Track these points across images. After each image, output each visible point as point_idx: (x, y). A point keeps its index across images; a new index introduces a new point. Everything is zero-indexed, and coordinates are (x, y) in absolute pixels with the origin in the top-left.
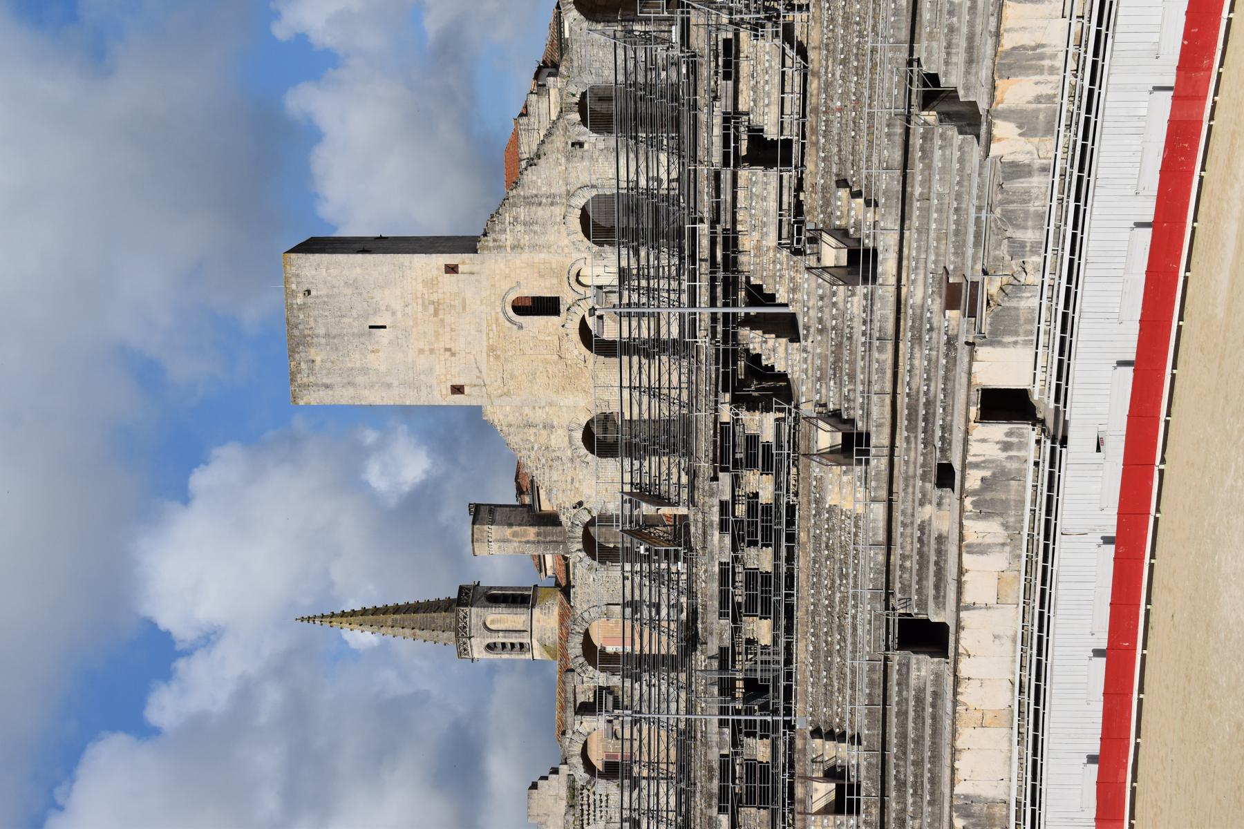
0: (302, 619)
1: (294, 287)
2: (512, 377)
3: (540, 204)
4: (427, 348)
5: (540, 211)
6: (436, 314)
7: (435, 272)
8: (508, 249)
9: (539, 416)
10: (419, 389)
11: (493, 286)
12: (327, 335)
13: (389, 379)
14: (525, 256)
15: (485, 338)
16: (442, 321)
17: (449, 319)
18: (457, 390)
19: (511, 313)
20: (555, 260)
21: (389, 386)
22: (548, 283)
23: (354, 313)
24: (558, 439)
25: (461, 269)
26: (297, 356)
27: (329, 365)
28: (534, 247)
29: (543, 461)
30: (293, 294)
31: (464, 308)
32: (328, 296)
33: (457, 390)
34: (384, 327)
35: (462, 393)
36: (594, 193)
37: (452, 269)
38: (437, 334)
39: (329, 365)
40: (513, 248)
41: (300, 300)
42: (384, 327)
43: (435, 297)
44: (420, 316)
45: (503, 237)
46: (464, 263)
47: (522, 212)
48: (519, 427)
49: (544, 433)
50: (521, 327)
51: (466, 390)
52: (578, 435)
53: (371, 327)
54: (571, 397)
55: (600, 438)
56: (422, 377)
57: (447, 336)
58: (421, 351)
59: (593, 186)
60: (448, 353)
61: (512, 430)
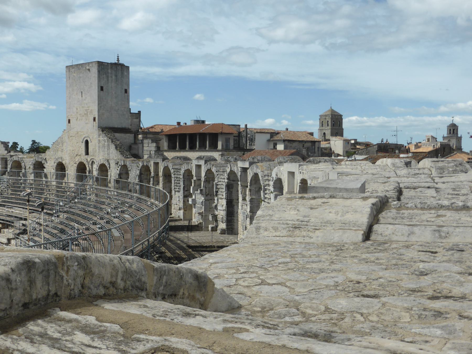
0: (118, 59)
5: (106, 150)
6: (85, 114)
9: (64, 148)
12: (80, 77)
14: (97, 144)
16: (83, 116)
17: (84, 118)
19: (85, 139)
24: (59, 154)
28: (99, 147)
30: (88, 66)
31: (86, 124)
36: (108, 168)
37: (94, 119)
38: (80, 114)
41: (88, 68)
43: (88, 114)
45: (101, 137)
47: (106, 144)
50: (82, 142)
52: (60, 161)
55: (61, 167)
58: (77, 109)
59: (110, 168)
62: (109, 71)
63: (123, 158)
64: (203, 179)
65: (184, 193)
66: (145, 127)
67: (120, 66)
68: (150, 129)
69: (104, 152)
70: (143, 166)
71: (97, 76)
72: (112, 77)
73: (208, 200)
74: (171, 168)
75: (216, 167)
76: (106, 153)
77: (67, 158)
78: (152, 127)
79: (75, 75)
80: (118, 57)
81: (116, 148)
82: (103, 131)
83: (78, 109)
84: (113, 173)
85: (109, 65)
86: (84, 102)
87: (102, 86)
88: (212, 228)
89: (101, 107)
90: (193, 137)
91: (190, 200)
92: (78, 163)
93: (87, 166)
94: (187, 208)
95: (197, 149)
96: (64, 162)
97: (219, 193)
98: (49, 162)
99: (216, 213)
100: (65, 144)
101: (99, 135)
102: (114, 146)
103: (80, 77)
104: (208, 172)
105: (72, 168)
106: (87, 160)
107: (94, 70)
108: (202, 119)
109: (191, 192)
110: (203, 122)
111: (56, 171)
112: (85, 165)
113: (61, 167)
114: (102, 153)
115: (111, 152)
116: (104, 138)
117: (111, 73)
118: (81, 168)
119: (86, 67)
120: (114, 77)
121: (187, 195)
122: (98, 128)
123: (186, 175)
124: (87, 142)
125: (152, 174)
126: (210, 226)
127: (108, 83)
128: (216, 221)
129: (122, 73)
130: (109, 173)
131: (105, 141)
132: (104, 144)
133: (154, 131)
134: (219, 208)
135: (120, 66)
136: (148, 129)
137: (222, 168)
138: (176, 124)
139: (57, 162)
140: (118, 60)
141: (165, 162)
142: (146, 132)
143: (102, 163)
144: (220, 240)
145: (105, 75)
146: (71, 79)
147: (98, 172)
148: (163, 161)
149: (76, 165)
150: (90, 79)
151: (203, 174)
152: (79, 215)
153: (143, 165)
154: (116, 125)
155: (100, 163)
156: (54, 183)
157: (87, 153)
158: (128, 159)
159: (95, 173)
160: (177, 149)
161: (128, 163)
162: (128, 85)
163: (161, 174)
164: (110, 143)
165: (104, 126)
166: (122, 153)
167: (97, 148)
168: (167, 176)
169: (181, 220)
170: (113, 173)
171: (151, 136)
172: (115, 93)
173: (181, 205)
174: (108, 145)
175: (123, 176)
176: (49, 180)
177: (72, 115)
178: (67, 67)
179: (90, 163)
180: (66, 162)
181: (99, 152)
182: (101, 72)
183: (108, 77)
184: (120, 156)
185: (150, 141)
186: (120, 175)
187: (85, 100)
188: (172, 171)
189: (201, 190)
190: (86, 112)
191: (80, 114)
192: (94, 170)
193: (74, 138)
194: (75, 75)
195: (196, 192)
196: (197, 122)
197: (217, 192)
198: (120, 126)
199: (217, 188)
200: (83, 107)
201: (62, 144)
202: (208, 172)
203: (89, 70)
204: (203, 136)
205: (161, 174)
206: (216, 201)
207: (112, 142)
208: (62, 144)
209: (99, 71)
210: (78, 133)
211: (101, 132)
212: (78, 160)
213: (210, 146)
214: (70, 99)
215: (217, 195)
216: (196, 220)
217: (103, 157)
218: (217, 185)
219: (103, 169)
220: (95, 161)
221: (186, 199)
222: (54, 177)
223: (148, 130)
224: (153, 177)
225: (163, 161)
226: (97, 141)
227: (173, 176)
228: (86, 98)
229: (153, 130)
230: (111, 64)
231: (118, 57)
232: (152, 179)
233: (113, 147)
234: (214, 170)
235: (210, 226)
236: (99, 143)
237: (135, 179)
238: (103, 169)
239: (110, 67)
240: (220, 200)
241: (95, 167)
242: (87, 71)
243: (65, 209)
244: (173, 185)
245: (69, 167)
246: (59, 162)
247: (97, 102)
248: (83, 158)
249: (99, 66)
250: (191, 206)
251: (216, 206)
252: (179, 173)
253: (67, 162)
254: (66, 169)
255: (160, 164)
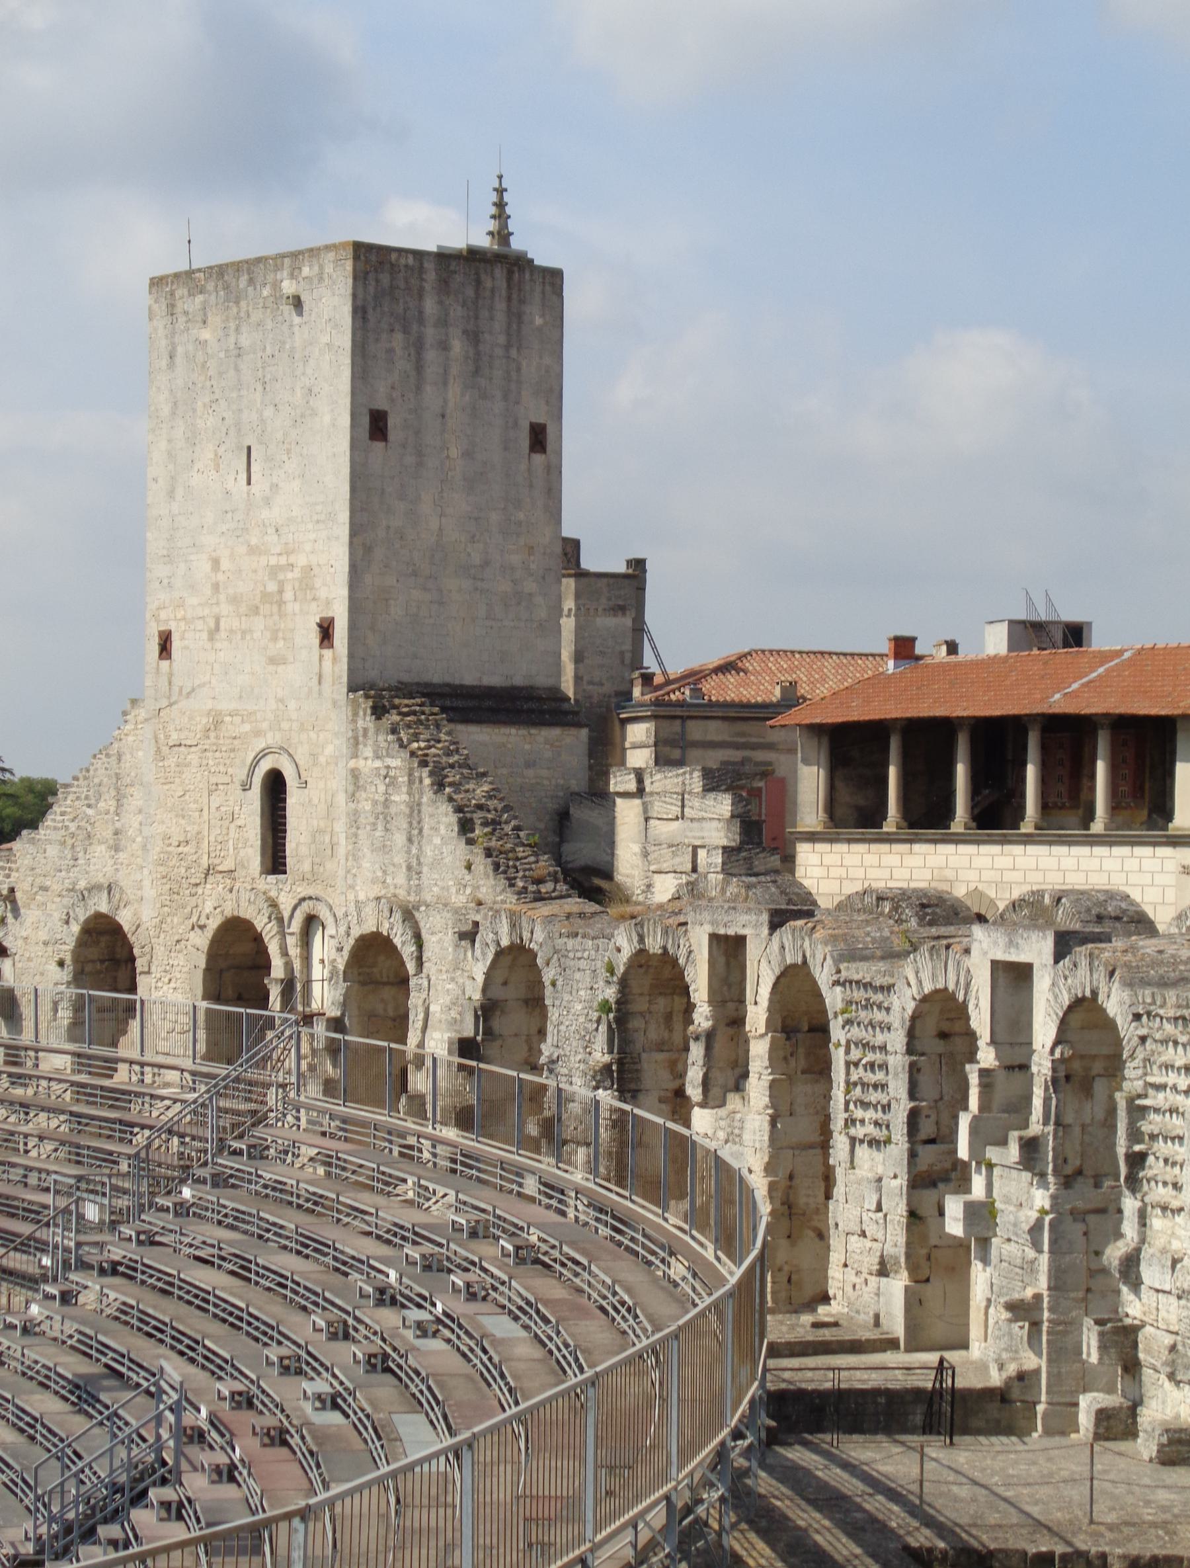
0: (501, 205)
1: (306, 271)
2: (182, 765)
3: (410, 840)
4: (221, 577)
5: (400, 839)
6: (265, 596)
7: (323, 593)
8: (352, 764)
9: (131, 821)
10: (169, 559)
11: (302, 728)
12: (239, 352)
13: (180, 492)
14: (341, 798)
15: (233, 706)
16: (255, 610)
17: (258, 623)
18: (165, 647)
19: (265, 766)
20: (335, 867)
21: (171, 494)
22: (304, 850)
23: (269, 412)
24: (99, 864)
25: (328, 653)
26: (210, 286)
27: (200, 357)
28: (354, 819)
29: (73, 827)
31: (273, 661)
32: (293, 349)
33: (165, 647)
34: (249, 483)
35: (161, 657)
36: (411, 967)
37: (326, 632)
38: (234, 600)
39: (200, 357)
40: (355, 774)
41: (288, 287)
42: (249, 483)
43: (288, 595)
44: (263, 560)
45: (368, 752)
46: (335, 660)
47: (400, 798)
48: (118, 777)
49: (108, 834)
50: (246, 787)
51: (165, 664)
52: (104, 908)
53: (249, 448)
54: (153, 893)
55: (106, 955)
56: (182, 566)
57: (235, 624)
58: (216, 563)
60: (212, 625)
61: (113, 760)
62: (430, 305)
63: (510, 900)
64: (1042, 1066)
65: (912, 1155)
66: (675, 669)
67: (499, 272)
68: (706, 686)
69: (386, 855)
70: (641, 958)
71: (344, 340)
72: (444, 346)
73: (1078, 1215)
74: (823, 976)
75: (1129, 984)
76: (399, 859)
77: (149, 892)
78: (727, 667)
79: (206, 335)
80: (500, 191)
81: (465, 827)
82: (379, 711)
83: (225, 564)
84: (445, 997)
85: (429, 265)
86: (265, 514)
87: (381, 404)
88: (1103, 1416)
89: (368, 549)
90: (997, 741)
91: (954, 1207)
92: (214, 924)
93: (273, 949)
94: (935, 1264)
95: (1027, 827)
96: (125, 919)
97: (1154, 1167)
98: (30, 915)
99: (1133, 1307)
100: (136, 799)
101: (355, 742)
102: (453, 819)
103: (239, 352)
104: (1076, 1019)
105: (179, 960)
106: (274, 905)
107: (332, 303)
108: (1070, 614)
109: (963, 1152)
110: (1075, 634)
111: (78, 978)
112: (258, 939)
113: (106, 955)
114: (369, 863)
115: (428, 851)
116: (383, 761)
117: (443, 322)
118: (237, 964)
119: (276, 286)
120: (458, 346)
121: (933, 1174)
122: (352, 689)
123: (930, 1026)
124: (275, 786)
125: (703, 1017)
126: (1088, 1405)
127: (419, 389)
128: (1132, 1367)
129: (516, 317)
130: (415, 1000)
131: (392, 783)
132: (387, 803)
133: (731, 696)
134: (1151, 1274)
135: (499, 272)
136: (694, 677)
137: (1171, 996)
138: (885, 647)
139: (82, 915)
140: (501, 211)
141: (785, 934)
142: (681, 704)
143: (369, 927)
144: (1148, 1514)
145: (399, 337)
146: (179, 360)
147: (343, 986)
148: (774, 926)
149: (202, 940)
150: (306, 359)
151: (1044, 1031)
152: (201, 1300)
153: (642, 952)
154: (472, 671)
155: (356, 932)
156: (62, 1062)
157: (275, 862)
158: (545, 909)
159: (325, 996)
160: (889, 826)
161: (539, 936)
162: (552, 391)
163: (757, 1016)
164: (428, 796)
165: (394, 675)
166: (501, 864)
167: (340, 827)
168: (803, 1029)
169: (891, 1344)
170: (445, 997)
171: (714, 730)
172: (468, 454)
173: (895, 1240)
174: (415, 809)
175: (511, 1022)
176: (27, 1037)
177: (181, 604)
178: (157, 283)
179: (296, 926)
180: (138, 916)
181: (354, 855)
182: (371, 315)
183: (419, 346)
184: (489, 886)
185: (695, 781)
186: (487, 1010)
187: (267, 502)
188: (834, 998)
189: (1031, 1147)
190: (272, 587)
191: (234, 600)
192: (317, 972)
193: (193, 757)
194: (206, 335)
195: (992, 1153)
196: (1031, 633)
197: (1137, 1160)
198: (494, 680)
199: (1135, 1135)
200: (253, 551)
201: (119, 800)
202: (1076, 1019)
203: (297, 303)
204: (1069, 737)
205: (757, 1016)
206: (1129, 1228)
207: (439, 786)
208: (119, 800)
209: (360, 312)
210: (218, 723)
211: (366, 721)
212: (215, 905)
213: (1116, 805)
214: (171, 494)
215: (1133, 1183)
216: (988, 1353)
217: (377, 890)
218: (1137, 1112)
219: (378, 968)
220: (324, 913)
221: (928, 1197)
222: (65, 1015)
223: (696, 692)
224: (710, 1036)
225: (774, 926)
226: (338, 783)
227: (837, 1033)
228: (275, 487)
229: (729, 690)
230: (444, 258)
231: (500, 191)
232: (697, 1051)
233: (441, 819)
234: (1116, 1003)
235: (1088, 1405)
236: (352, 797)
237: (587, 1047)
238: (378, 968)
239: (431, 276)
240: (1157, 1222)
241: (328, 953)
242: (287, 310)
243: (117, 1253)
244: (838, 1094)
245: (160, 951)
246: (98, 916)
247: (344, 516)
248: (248, 895)
249: (360, 277)
250: (960, 1247)
251: (1131, 1264)
252: (879, 1016)
253: (148, 914)
254: (140, 964)
255: (752, 951)
